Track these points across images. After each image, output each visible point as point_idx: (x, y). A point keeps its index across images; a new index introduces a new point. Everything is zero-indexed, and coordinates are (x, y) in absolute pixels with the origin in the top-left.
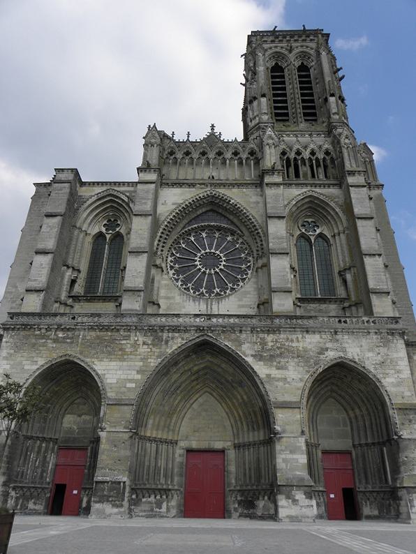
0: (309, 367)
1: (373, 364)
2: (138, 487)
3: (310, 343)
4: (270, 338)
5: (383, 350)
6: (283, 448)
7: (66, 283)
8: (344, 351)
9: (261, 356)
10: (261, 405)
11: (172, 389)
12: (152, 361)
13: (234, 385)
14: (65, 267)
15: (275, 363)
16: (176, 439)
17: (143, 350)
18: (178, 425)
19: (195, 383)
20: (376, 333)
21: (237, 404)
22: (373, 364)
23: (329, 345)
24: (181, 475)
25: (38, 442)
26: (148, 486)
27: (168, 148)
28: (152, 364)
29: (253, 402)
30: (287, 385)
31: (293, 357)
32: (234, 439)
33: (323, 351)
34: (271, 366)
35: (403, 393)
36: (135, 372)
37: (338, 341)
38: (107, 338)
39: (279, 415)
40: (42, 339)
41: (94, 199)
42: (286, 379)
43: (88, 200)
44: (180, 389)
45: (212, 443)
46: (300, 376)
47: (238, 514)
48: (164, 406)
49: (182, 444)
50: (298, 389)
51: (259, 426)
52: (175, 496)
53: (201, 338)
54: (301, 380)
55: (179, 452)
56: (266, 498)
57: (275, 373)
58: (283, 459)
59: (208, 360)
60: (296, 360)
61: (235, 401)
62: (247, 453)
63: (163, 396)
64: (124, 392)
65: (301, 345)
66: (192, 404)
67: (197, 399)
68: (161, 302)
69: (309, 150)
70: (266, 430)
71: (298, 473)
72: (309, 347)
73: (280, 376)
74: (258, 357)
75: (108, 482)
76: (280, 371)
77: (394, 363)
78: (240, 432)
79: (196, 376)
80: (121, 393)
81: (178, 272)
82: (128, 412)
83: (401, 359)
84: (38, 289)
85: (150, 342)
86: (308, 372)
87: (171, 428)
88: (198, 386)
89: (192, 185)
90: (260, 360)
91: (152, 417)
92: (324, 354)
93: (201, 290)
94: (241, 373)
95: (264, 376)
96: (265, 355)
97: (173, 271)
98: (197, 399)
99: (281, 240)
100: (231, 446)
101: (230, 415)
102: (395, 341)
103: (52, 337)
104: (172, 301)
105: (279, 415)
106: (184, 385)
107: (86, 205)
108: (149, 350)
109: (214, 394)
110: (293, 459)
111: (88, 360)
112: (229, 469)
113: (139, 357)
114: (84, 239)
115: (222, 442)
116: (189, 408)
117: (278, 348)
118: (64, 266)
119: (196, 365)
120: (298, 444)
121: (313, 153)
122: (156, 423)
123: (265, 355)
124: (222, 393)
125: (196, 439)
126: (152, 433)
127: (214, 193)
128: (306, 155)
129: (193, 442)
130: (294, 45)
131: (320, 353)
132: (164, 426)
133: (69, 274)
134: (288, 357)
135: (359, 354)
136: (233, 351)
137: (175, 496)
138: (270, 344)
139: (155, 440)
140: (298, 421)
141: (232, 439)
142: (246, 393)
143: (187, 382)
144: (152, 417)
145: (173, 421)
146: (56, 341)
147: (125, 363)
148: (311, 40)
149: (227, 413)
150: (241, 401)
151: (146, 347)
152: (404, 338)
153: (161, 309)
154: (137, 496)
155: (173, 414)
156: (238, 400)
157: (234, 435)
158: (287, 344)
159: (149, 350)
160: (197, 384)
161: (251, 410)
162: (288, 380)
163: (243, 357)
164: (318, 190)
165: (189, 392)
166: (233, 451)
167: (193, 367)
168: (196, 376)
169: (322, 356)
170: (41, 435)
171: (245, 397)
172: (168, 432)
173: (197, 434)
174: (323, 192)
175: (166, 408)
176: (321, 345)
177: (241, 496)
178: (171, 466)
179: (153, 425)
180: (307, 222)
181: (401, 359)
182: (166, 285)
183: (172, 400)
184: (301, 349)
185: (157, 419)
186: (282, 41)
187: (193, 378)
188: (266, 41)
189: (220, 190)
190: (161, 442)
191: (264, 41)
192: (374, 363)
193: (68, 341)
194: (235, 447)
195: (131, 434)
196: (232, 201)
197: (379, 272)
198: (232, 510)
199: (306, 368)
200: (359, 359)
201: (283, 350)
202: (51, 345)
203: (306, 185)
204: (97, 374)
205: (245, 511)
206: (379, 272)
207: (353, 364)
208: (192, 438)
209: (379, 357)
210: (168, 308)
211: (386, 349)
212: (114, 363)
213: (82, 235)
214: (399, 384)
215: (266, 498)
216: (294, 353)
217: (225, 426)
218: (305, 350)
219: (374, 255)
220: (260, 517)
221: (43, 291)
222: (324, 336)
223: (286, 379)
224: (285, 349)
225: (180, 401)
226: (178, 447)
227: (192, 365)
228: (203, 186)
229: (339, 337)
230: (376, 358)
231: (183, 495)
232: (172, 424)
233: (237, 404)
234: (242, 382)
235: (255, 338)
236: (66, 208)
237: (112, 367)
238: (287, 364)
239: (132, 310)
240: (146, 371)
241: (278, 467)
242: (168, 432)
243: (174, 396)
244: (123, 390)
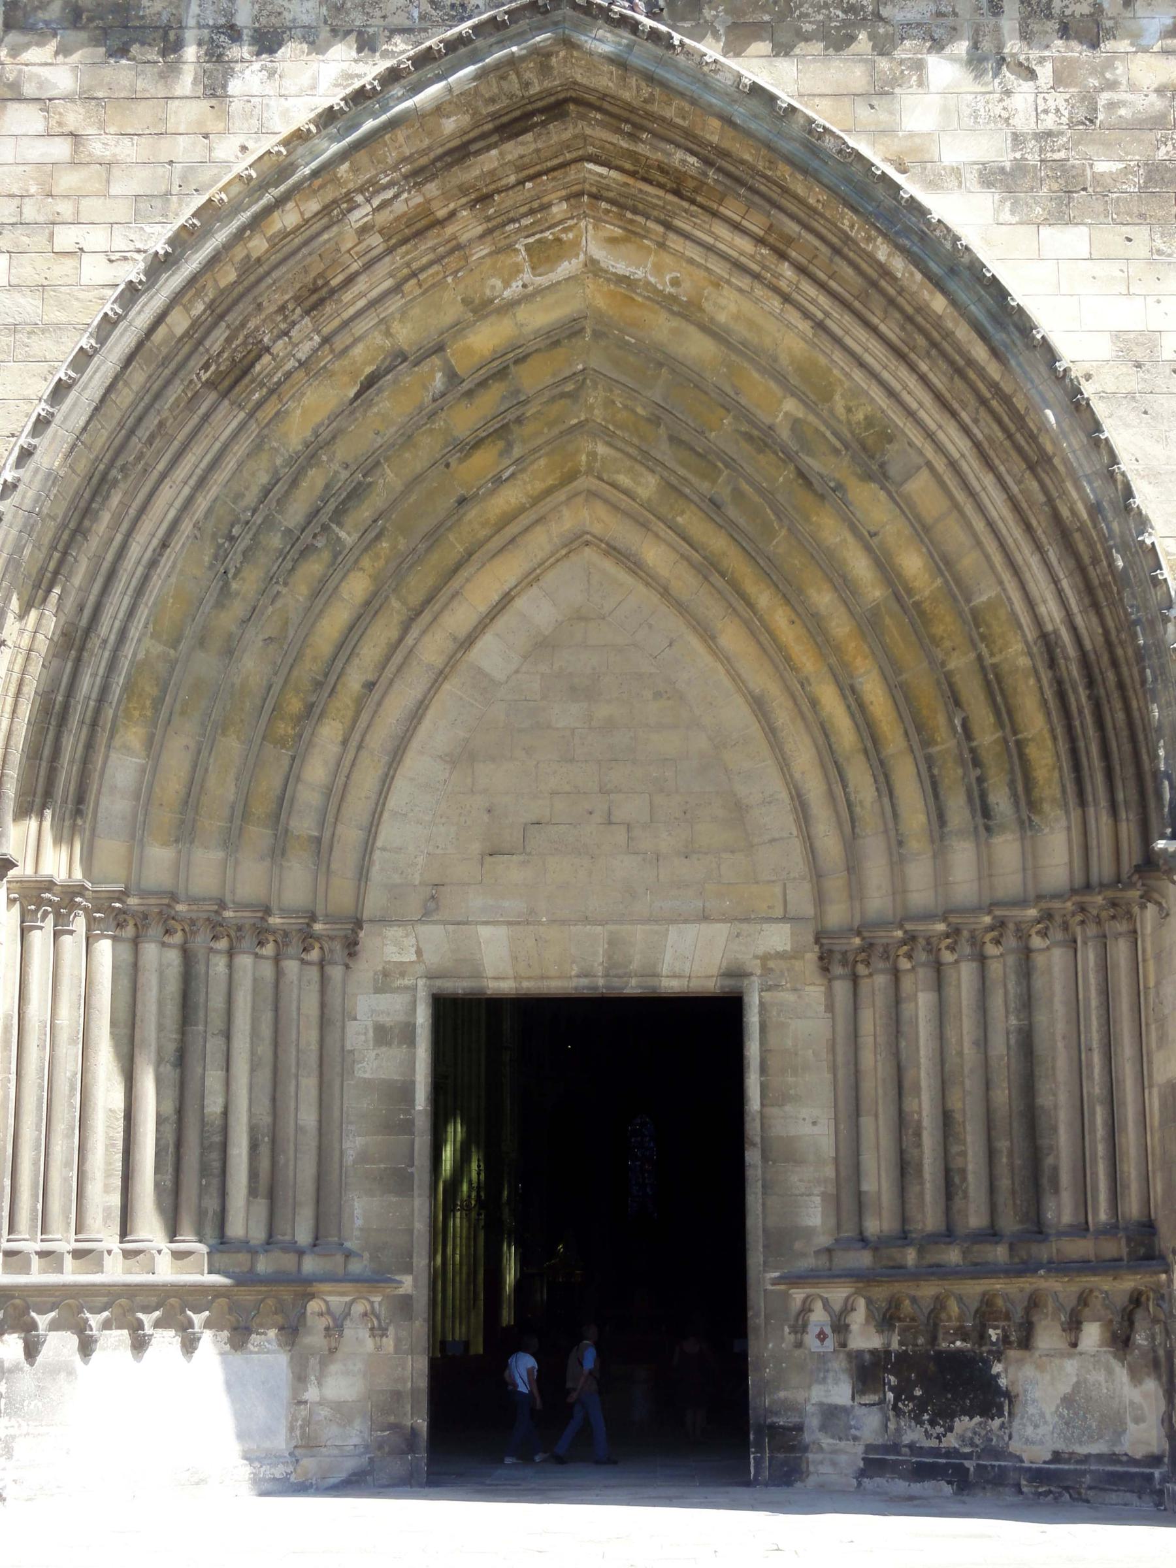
2: (37, 1276)
10: (1050, 610)
11: (295, 512)
12: (96, 239)
13: (814, 464)
16: (341, 895)
19: (484, 460)
21: (841, 627)
24: (399, 1182)
26: (115, 1272)
28: (96, 271)
29: (981, 599)
32: (820, 899)
44: (364, 512)
45: (639, 934)
47: (852, 1454)
48: (230, 651)
51: (1029, 783)
52: (358, 1338)
56: (1092, 1334)
59: (592, 266)
61: (823, 599)
62: (922, 1004)
63: (220, 556)
66: (469, 641)
67: (507, 599)
70: (1101, 821)
78: (874, 850)
79: (490, 401)
87: (303, 825)
91: (133, 736)
94: (875, 354)
95: (1103, 349)
98: (507, 599)
100: (796, 954)
101: (783, 715)
106: (390, 478)
109: (655, 555)
112: (779, 1129)
115: (720, 931)
116: (440, 677)
119: (482, 309)
122: (172, 785)
124: (718, 543)
125: (514, 906)
129: (485, 932)
132: (242, 813)
137: (358, 1338)
141: (801, 900)
142: (923, 531)
143: (418, 459)
144: (133, 736)
145: (316, 771)
149: (758, 705)
150: (875, 593)
154: (31, 1351)
155: (311, 714)
156: (845, 586)
157: (817, 875)
159: (60, 149)
161: (960, 662)
163: (911, 187)
165: (434, 537)
166: (815, 993)
167: (458, 328)
168: (490, 401)
171: (912, 564)
172: (278, 851)
173: (512, 871)
177: (886, 1319)
178: (308, 1117)
183: (299, 591)
190: (216, 927)
194: (825, 961)
198: (813, 1422)
205: (914, 1434)
208: (476, 901)
215: (1092, 1334)
217: (738, 811)
220: (1039, 1475)
225: (370, 609)
226: (366, 968)
227: (452, 311)
231: (420, 1326)
232: (309, 796)
233: (841, 627)
234: (888, 436)
240: (38, 329)
242: (278, 851)
243: (314, 567)
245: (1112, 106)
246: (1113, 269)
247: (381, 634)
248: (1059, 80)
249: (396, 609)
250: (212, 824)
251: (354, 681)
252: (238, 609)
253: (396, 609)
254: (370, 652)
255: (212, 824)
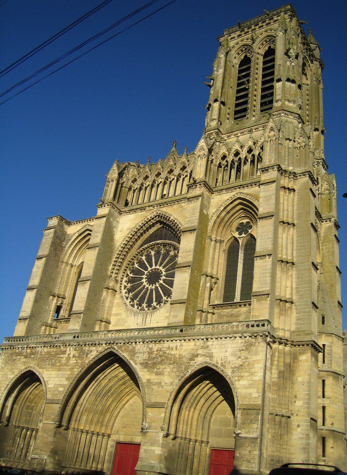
0: (180, 373)
1: (232, 368)
3: (185, 350)
4: (155, 347)
5: (244, 354)
6: (147, 441)
7: (52, 310)
8: (211, 356)
9: (147, 363)
11: (103, 393)
14: (52, 297)
15: (155, 370)
17: (73, 361)
18: (112, 422)
20: (241, 337)
22: (232, 368)
23: (200, 352)
25: (24, 430)
27: (132, 177)
30: (161, 389)
31: (170, 364)
33: (194, 356)
34: (152, 372)
35: (251, 394)
36: (65, 379)
37: (208, 347)
38: (53, 353)
39: (150, 414)
40: (19, 356)
41: (76, 235)
42: (161, 383)
43: (72, 237)
46: (171, 381)
49: (114, 437)
50: (168, 392)
53: (109, 351)
54: (172, 384)
55: (111, 443)
57: (154, 378)
58: (145, 449)
60: (171, 366)
64: (57, 394)
65: (178, 352)
68: (113, 319)
69: (246, 149)
71: (152, 462)
72: (184, 355)
73: (156, 381)
74: (145, 365)
75: (37, 459)
76: (158, 376)
77: (251, 366)
79: (123, 381)
80: (55, 395)
81: (129, 291)
82: (57, 408)
83: (258, 361)
84: (25, 318)
85: (77, 355)
86: (178, 376)
87: (105, 424)
88: (127, 390)
89: (142, 209)
90: (145, 368)
91: (86, 414)
92: (194, 360)
93: (143, 305)
96: (150, 362)
97: (126, 290)
99: (187, 254)
102: (257, 344)
103: (25, 354)
104: (119, 317)
105: (150, 414)
106: (113, 389)
107: (71, 242)
108: (75, 362)
110: (152, 450)
111: (40, 370)
113: (69, 367)
114: (70, 271)
117: (160, 356)
118: (51, 295)
120: (157, 438)
121: (250, 151)
122: (90, 419)
123: (150, 362)
125: (124, 433)
126: (85, 426)
127: (159, 212)
128: (243, 154)
130: (258, 32)
131: (191, 359)
132: (97, 423)
133: (54, 303)
134: (166, 364)
135: (223, 358)
136: (128, 360)
138: (155, 353)
139: (87, 432)
140: (161, 419)
144: (86, 414)
145: (107, 418)
146: (26, 357)
147: (60, 372)
148: (275, 21)
151: (74, 359)
152: (266, 341)
153: (111, 325)
158: (167, 352)
160: (126, 388)
162: (162, 384)
164: (246, 190)
169: (192, 362)
170: (26, 426)
173: (125, 430)
174: (248, 192)
175: (100, 408)
176: (194, 352)
179: (87, 420)
180: (243, 223)
181: (258, 361)
182: (118, 304)
184: (177, 356)
185: (91, 417)
186: (248, 32)
187: (120, 383)
188: (234, 38)
189: (161, 209)
191: (232, 38)
192: (233, 366)
193: (32, 356)
195: (55, 425)
196: (172, 218)
197: (266, 273)
199: (178, 373)
200: (221, 363)
201: (163, 358)
202: (23, 360)
203: (235, 188)
204: (44, 380)
206: (266, 273)
207: (215, 368)
209: (240, 362)
210: (116, 325)
211: (247, 352)
212: (54, 372)
213: (68, 267)
214: (250, 386)
216: (171, 360)
218: (181, 357)
219: (265, 256)
221: (27, 319)
222: (198, 343)
223: (161, 383)
224: (166, 357)
228: (151, 208)
229: (210, 343)
230: (235, 362)
232: (106, 420)
235: (145, 348)
236: (50, 250)
237: (53, 375)
238: (164, 370)
239: (74, 330)
241: (140, 456)
242: (102, 426)
244: (57, 392)
245: (152, 356)
246: (149, 373)
247: (114, 404)
248: (148, 354)
249: (116, 402)
250: (94, 423)
251: (111, 409)
252: (98, 402)
253: (116, 402)
254: (113, 406)
255: (94, 423)
